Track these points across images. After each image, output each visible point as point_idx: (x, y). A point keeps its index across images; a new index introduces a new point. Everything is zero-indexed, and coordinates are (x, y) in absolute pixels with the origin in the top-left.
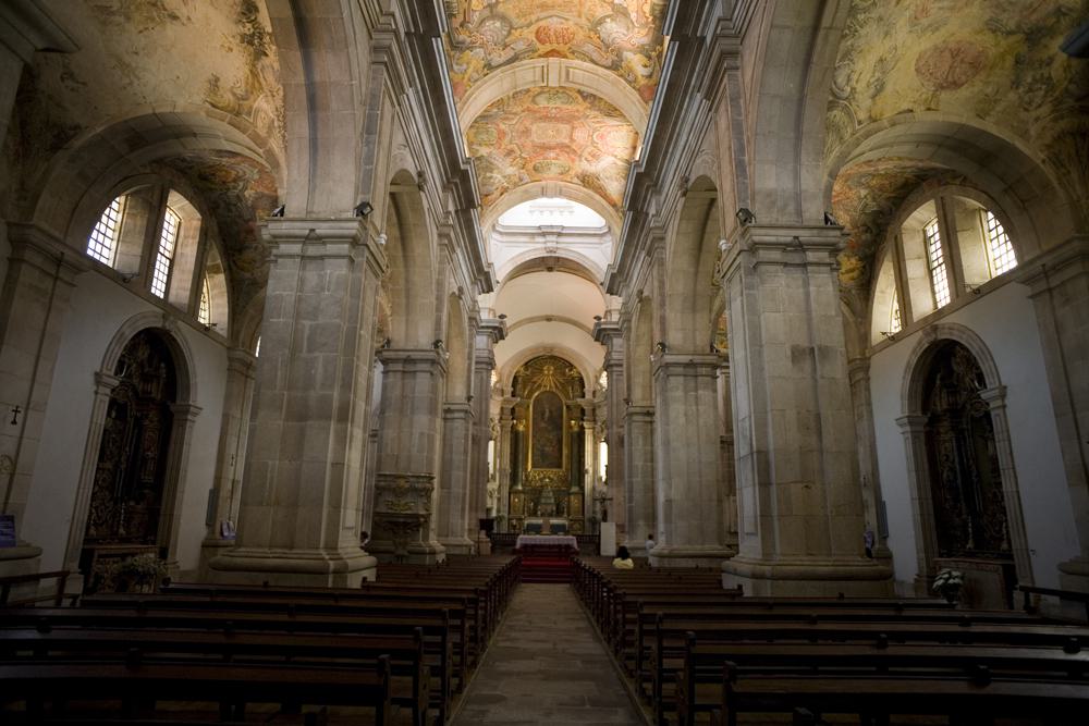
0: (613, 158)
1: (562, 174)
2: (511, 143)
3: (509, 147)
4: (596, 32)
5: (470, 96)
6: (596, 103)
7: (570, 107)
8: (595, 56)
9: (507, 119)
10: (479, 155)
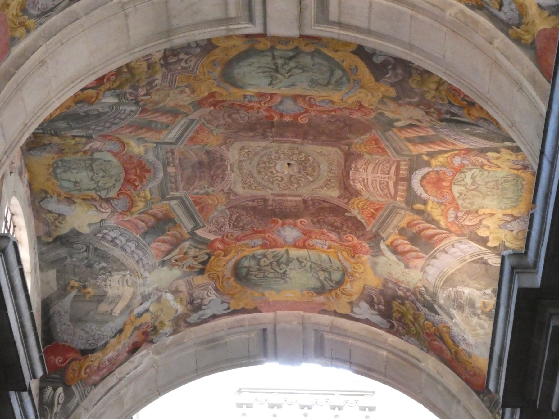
0: (477, 247)
1: (321, 290)
2: (163, 197)
3: (159, 208)
5: (25, 56)
6: (413, 84)
7: (336, 97)
9: (149, 126)
10: (64, 230)
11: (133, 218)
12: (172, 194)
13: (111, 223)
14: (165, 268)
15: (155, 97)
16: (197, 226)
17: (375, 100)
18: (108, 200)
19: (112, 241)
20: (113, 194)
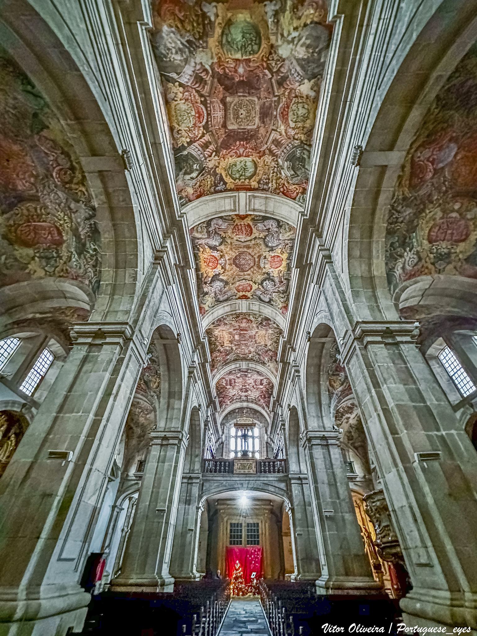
4: (222, 238)
8: (220, 222)
11: (291, 86)
12: (276, 99)
13: (297, 84)
14: (284, 57)
15: (273, 163)
16: (271, 79)
17: (221, 164)
18: (296, 97)
19: (299, 74)
20: (294, 99)
